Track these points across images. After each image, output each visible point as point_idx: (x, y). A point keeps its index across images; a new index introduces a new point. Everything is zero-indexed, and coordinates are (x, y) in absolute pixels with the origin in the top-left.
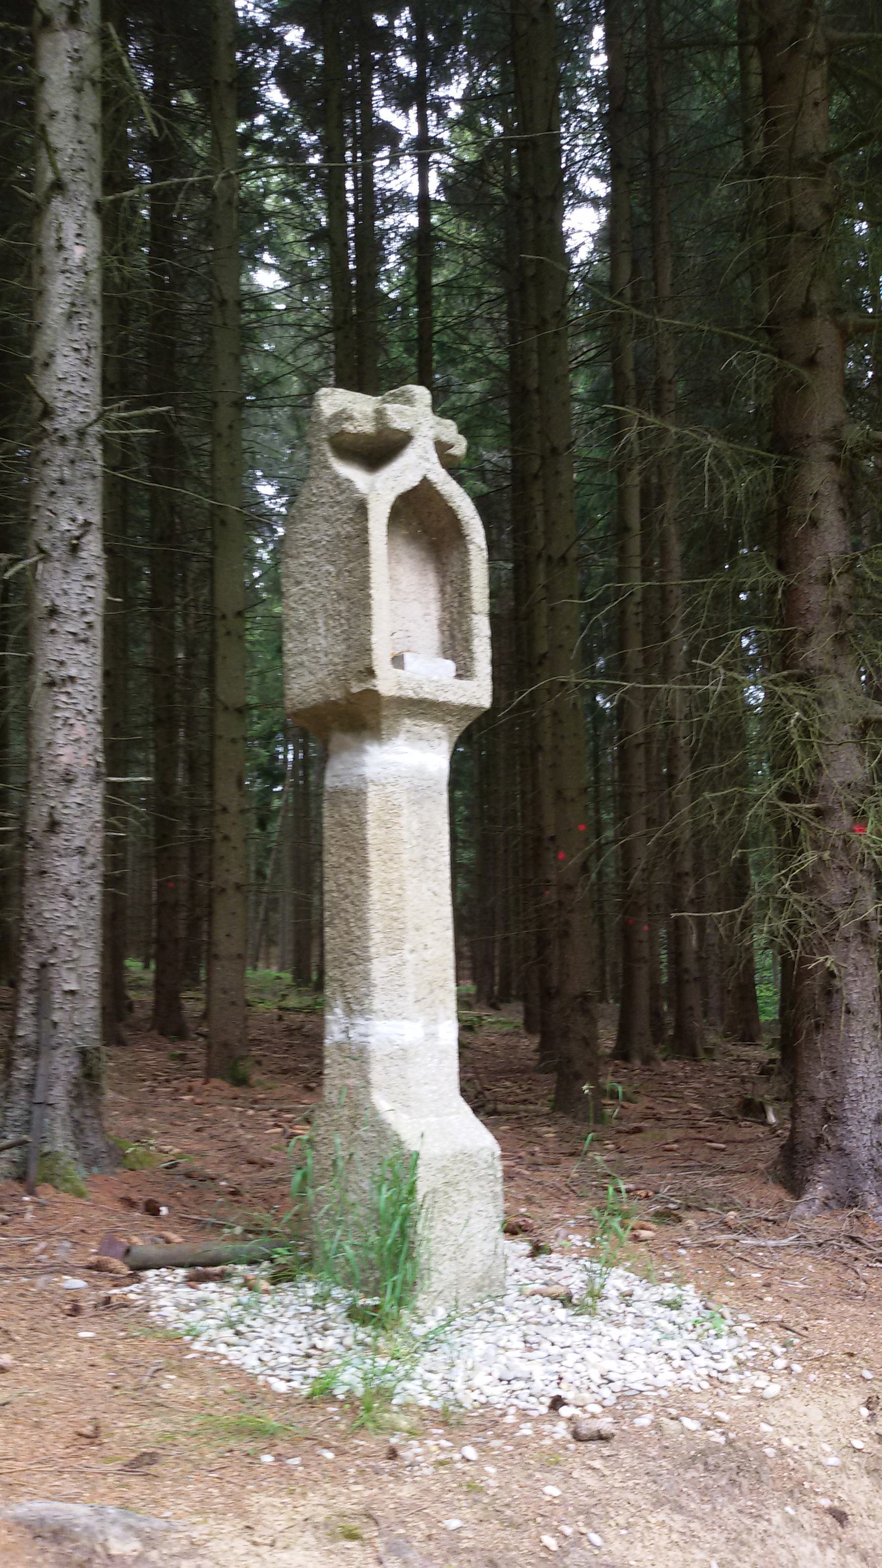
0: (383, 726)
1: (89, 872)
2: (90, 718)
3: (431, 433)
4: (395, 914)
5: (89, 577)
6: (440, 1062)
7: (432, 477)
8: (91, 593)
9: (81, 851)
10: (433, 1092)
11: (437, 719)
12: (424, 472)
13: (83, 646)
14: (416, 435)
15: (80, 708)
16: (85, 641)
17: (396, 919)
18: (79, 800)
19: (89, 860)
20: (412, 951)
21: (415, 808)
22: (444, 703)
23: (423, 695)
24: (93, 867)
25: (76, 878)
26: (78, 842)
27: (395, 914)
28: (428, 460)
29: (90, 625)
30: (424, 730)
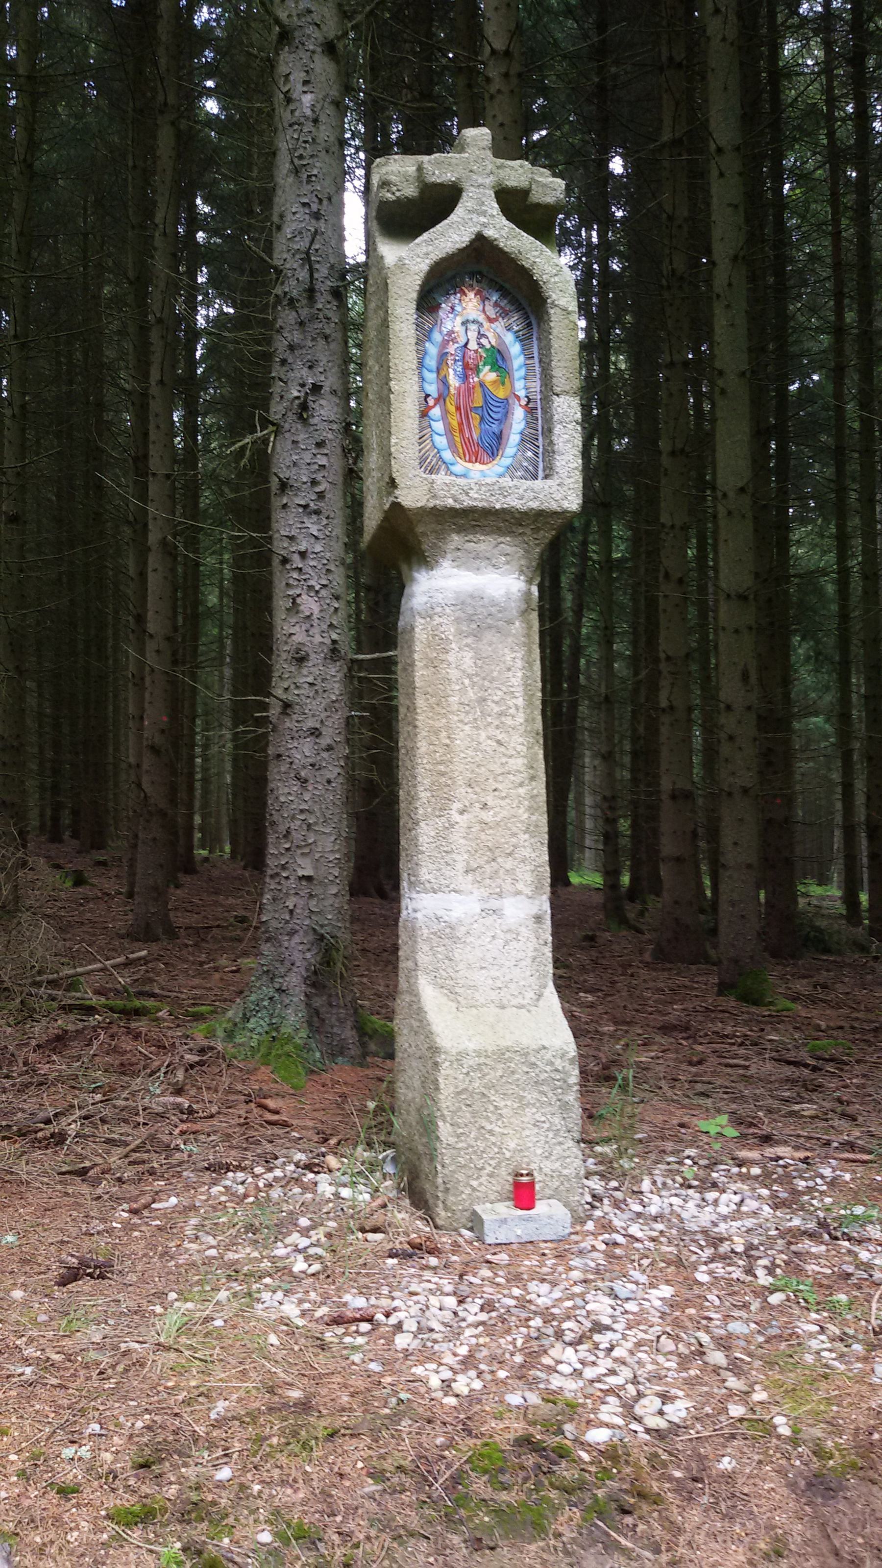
0: (424, 547)
1: (325, 755)
2: (324, 593)
3: (489, 181)
4: (442, 768)
5: (320, 445)
6: (507, 943)
7: (490, 233)
8: (323, 461)
9: (315, 733)
10: (494, 979)
11: (499, 532)
12: (477, 229)
13: (314, 518)
14: (465, 185)
15: (312, 583)
16: (317, 512)
17: (443, 774)
18: (310, 679)
19: (325, 741)
20: (462, 812)
21: (469, 640)
22: (503, 510)
23: (467, 503)
24: (329, 748)
25: (310, 760)
26: (311, 723)
27: (442, 768)
28: (484, 214)
29: (321, 495)
30: (482, 547)
